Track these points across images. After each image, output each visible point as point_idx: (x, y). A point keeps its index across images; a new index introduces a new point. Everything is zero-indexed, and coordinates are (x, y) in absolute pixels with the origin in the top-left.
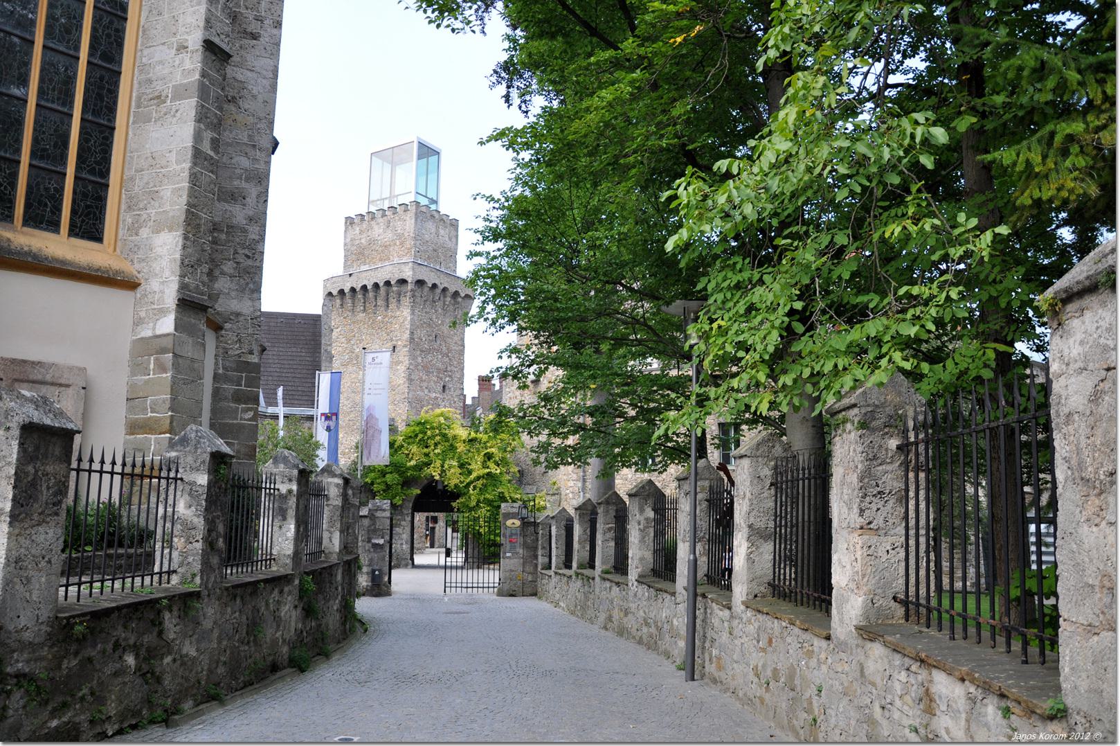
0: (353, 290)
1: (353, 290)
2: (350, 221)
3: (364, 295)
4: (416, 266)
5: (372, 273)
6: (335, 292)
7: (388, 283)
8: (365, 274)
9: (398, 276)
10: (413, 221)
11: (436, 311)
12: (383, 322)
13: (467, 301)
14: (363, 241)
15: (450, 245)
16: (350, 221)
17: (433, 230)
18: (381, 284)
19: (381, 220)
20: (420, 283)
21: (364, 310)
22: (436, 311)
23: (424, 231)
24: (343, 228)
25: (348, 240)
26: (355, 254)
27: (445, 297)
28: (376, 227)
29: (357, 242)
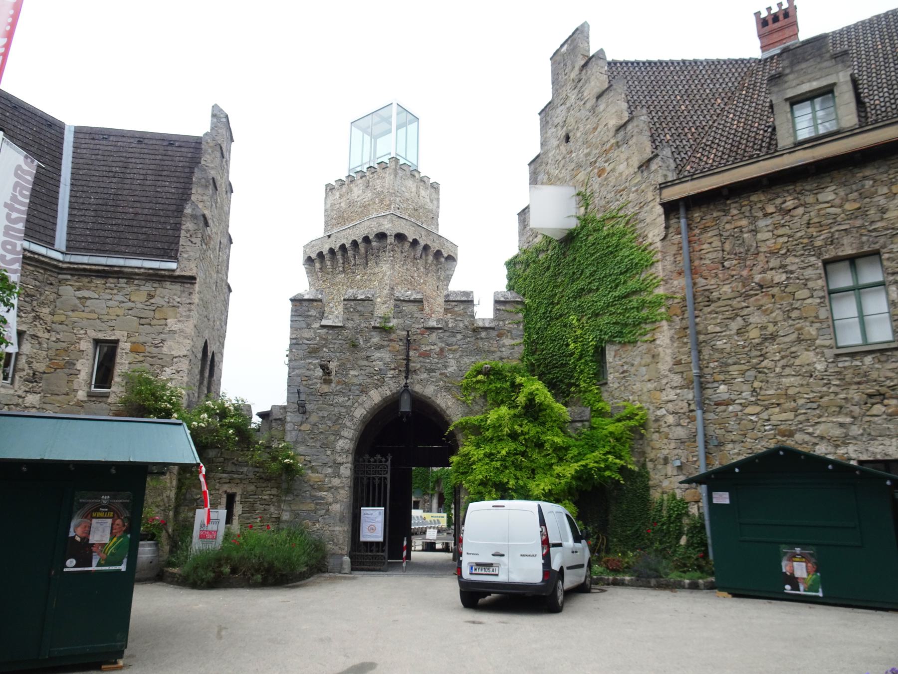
0: (332, 251)
1: (332, 251)
2: (330, 189)
3: (343, 255)
4: (394, 218)
5: (350, 231)
6: (314, 256)
7: (366, 239)
8: (343, 233)
9: (376, 230)
10: (392, 176)
11: (418, 269)
12: (362, 280)
13: (449, 262)
14: (342, 205)
15: (430, 206)
16: (330, 189)
17: (414, 190)
18: (360, 241)
19: (360, 181)
20: (400, 237)
21: (344, 271)
22: (418, 269)
23: (404, 189)
24: (324, 196)
25: (328, 206)
26: (335, 218)
27: (427, 255)
28: (355, 189)
29: (337, 206)
